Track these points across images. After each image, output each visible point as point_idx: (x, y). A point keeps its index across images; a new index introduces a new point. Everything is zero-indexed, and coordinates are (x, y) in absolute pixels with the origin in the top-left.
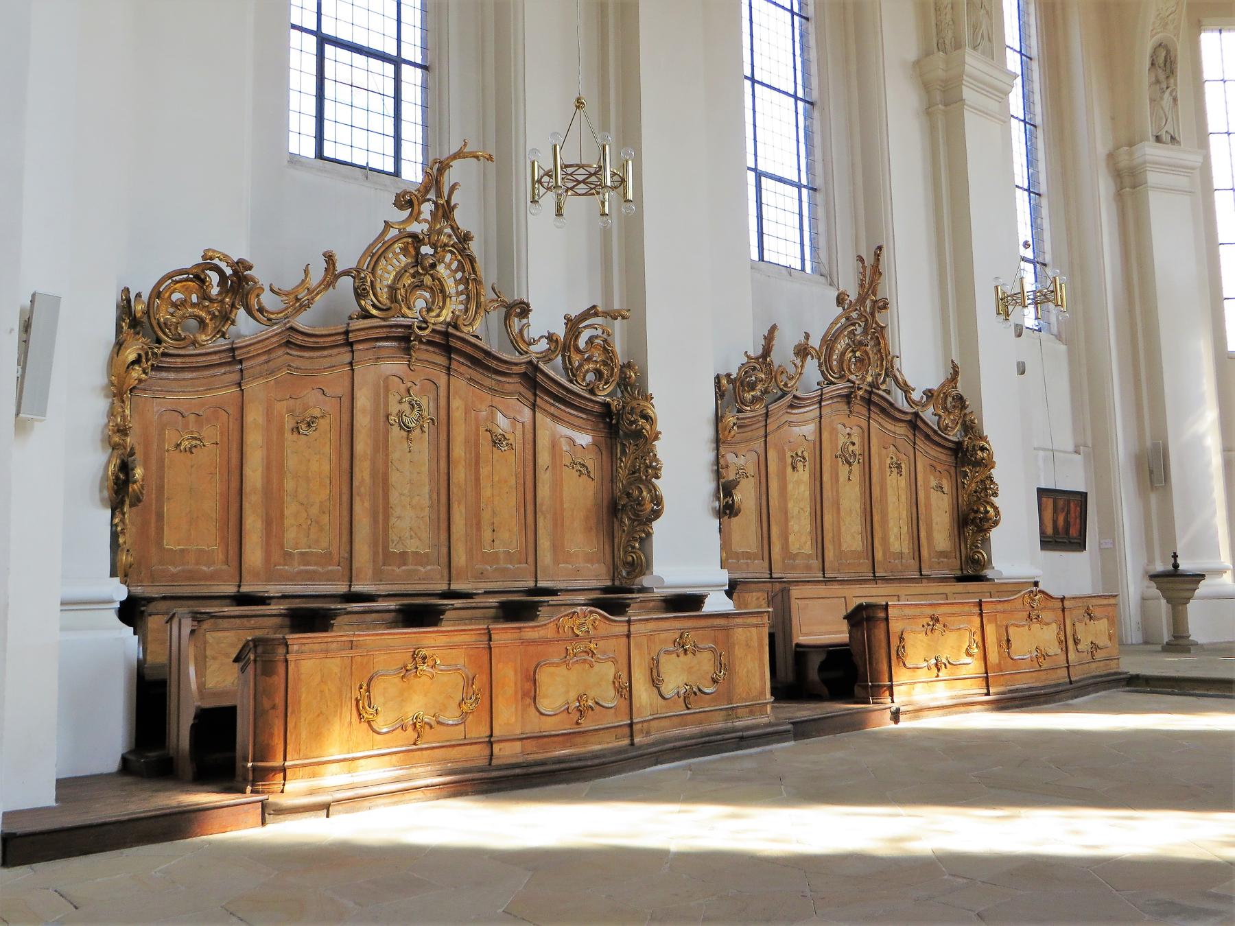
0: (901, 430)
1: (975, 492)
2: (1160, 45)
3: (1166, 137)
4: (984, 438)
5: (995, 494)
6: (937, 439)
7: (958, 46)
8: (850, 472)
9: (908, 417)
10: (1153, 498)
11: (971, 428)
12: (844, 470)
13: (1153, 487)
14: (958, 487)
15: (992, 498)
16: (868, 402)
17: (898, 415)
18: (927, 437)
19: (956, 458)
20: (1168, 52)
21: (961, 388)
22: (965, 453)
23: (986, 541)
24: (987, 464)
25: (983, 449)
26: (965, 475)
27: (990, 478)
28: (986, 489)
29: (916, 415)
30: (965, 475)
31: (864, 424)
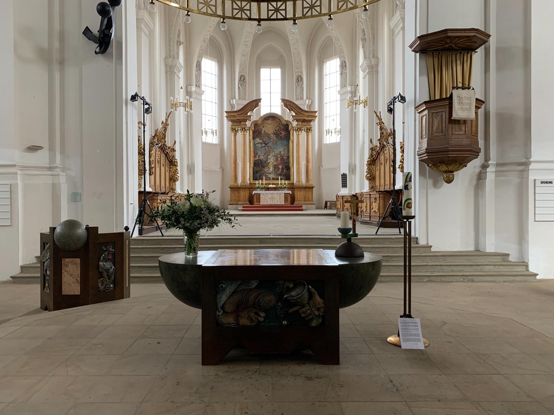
0: (164, 155)
1: (173, 172)
2: (198, 61)
3: (198, 86)
4: (176, 160)
5: (178, 173)
6: (169, 158)
7: (174, 58)
8: (158, 165)
9: (166, 153)
10: (190, 176)
11: (173, 156)
12: (158, 164)
13: (191, 173)
14: (170, 171)
15: (177, 174)
16: (161, 149)
17: (165, 152)
18: (168, 158)
19: (170, 163)
20: (200, 64)
21: (174, 147)
22: (172, 163)
23: (175, 184)
24: (176, 166)
25: (176, 162)
26: (171, 168)
27: (177, 169)
28: (176, 172)
29: (167, 152)
30: (171, 168)
31: (160, 154)
